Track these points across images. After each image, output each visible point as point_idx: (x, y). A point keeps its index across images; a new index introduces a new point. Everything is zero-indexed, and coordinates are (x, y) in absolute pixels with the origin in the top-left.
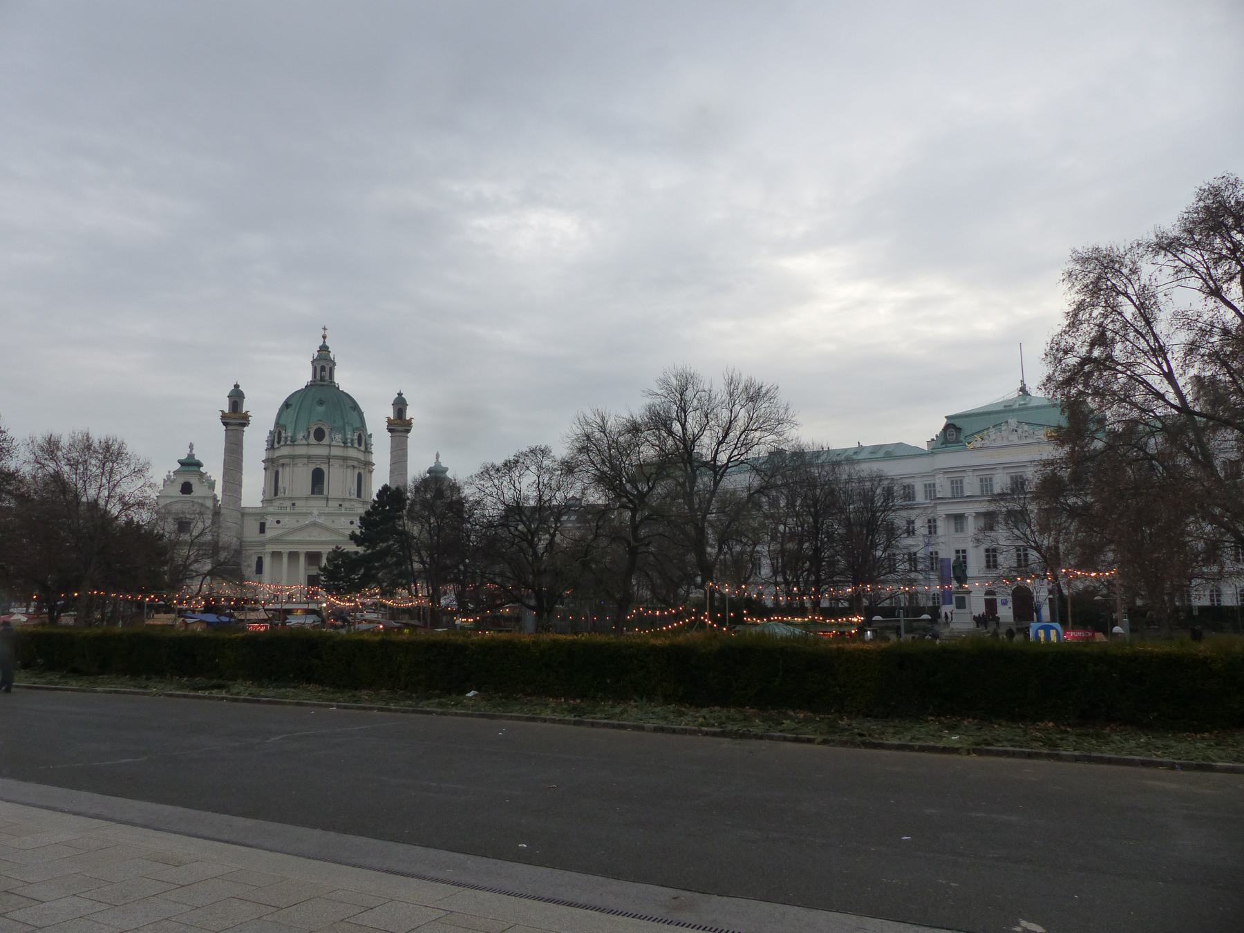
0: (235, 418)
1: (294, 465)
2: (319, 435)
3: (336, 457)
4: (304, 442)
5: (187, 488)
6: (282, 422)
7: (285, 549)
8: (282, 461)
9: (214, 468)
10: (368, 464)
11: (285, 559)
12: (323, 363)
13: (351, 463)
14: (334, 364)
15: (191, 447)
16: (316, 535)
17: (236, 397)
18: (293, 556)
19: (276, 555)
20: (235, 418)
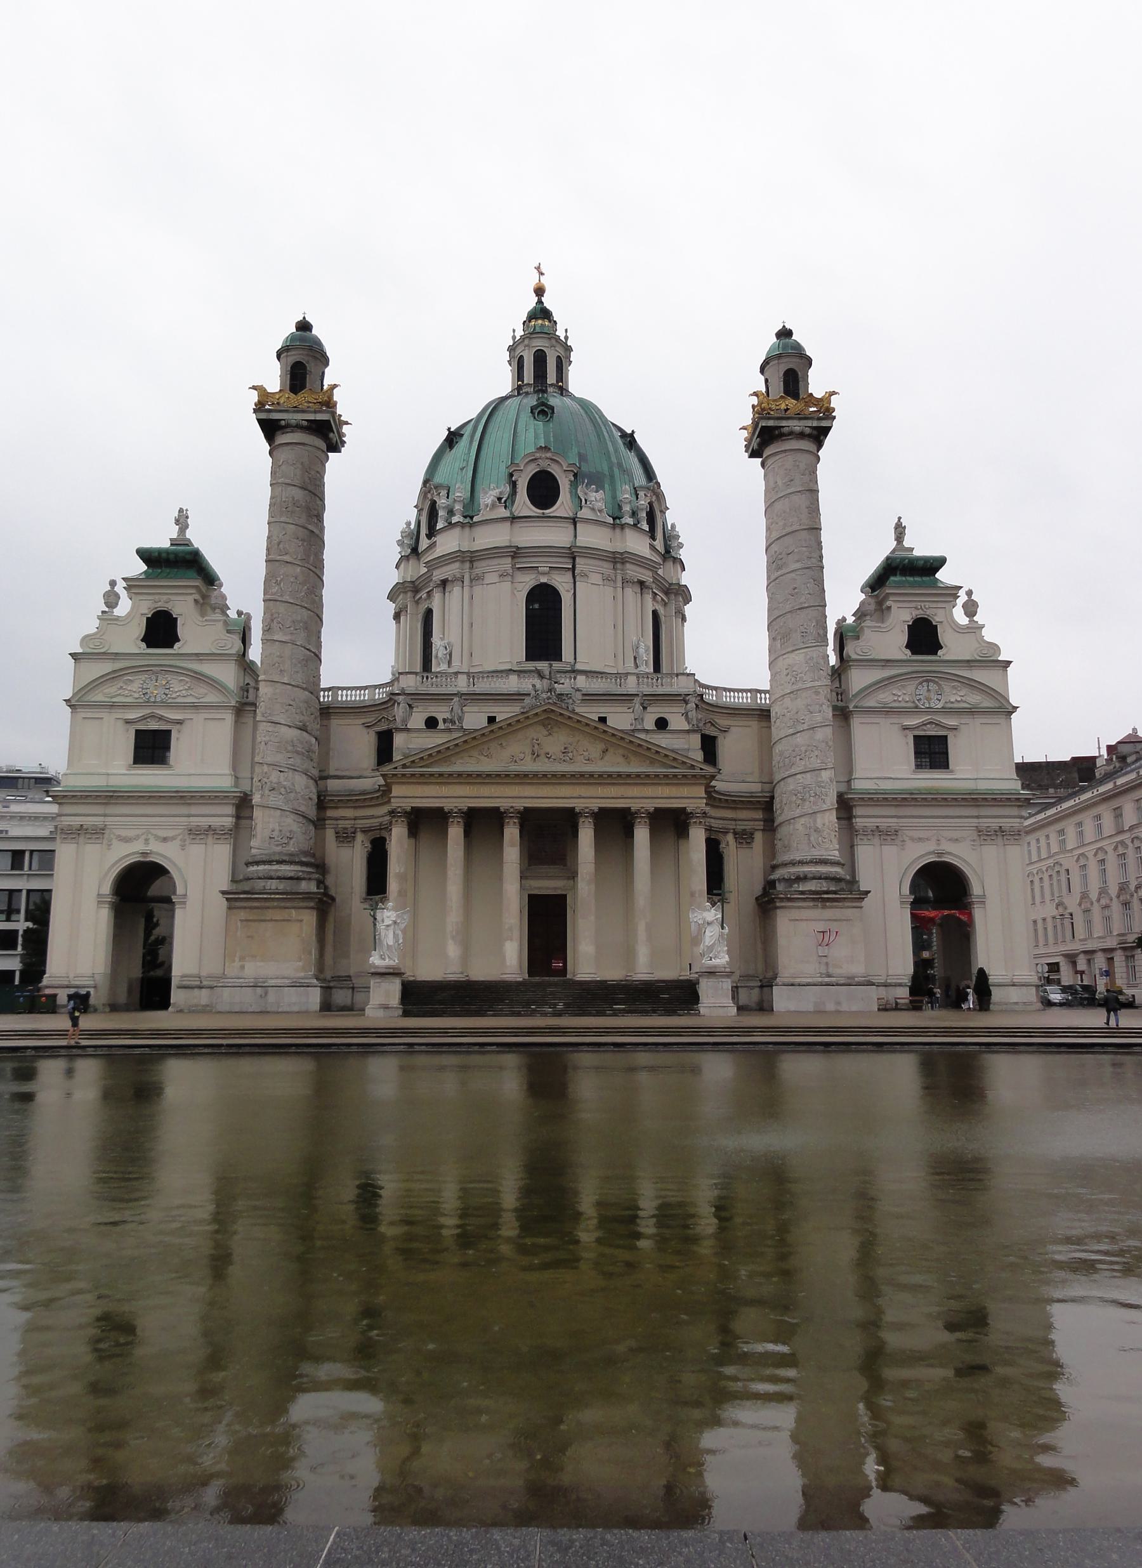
0: (301, 415)
1: (476, 579)
2: (543, 490)
4: (503, 512)
5: (161, 630)
6: (438, 479)
7: (455, 798)
8: (439, 575)
9: (243, 584)
11: (455, 832)
12: (539, 343)
14: (569, 349)
15: (182, 520)
16: (555, 750)
17: (303, 358)
18: (482, 824)
20: (301, 415)
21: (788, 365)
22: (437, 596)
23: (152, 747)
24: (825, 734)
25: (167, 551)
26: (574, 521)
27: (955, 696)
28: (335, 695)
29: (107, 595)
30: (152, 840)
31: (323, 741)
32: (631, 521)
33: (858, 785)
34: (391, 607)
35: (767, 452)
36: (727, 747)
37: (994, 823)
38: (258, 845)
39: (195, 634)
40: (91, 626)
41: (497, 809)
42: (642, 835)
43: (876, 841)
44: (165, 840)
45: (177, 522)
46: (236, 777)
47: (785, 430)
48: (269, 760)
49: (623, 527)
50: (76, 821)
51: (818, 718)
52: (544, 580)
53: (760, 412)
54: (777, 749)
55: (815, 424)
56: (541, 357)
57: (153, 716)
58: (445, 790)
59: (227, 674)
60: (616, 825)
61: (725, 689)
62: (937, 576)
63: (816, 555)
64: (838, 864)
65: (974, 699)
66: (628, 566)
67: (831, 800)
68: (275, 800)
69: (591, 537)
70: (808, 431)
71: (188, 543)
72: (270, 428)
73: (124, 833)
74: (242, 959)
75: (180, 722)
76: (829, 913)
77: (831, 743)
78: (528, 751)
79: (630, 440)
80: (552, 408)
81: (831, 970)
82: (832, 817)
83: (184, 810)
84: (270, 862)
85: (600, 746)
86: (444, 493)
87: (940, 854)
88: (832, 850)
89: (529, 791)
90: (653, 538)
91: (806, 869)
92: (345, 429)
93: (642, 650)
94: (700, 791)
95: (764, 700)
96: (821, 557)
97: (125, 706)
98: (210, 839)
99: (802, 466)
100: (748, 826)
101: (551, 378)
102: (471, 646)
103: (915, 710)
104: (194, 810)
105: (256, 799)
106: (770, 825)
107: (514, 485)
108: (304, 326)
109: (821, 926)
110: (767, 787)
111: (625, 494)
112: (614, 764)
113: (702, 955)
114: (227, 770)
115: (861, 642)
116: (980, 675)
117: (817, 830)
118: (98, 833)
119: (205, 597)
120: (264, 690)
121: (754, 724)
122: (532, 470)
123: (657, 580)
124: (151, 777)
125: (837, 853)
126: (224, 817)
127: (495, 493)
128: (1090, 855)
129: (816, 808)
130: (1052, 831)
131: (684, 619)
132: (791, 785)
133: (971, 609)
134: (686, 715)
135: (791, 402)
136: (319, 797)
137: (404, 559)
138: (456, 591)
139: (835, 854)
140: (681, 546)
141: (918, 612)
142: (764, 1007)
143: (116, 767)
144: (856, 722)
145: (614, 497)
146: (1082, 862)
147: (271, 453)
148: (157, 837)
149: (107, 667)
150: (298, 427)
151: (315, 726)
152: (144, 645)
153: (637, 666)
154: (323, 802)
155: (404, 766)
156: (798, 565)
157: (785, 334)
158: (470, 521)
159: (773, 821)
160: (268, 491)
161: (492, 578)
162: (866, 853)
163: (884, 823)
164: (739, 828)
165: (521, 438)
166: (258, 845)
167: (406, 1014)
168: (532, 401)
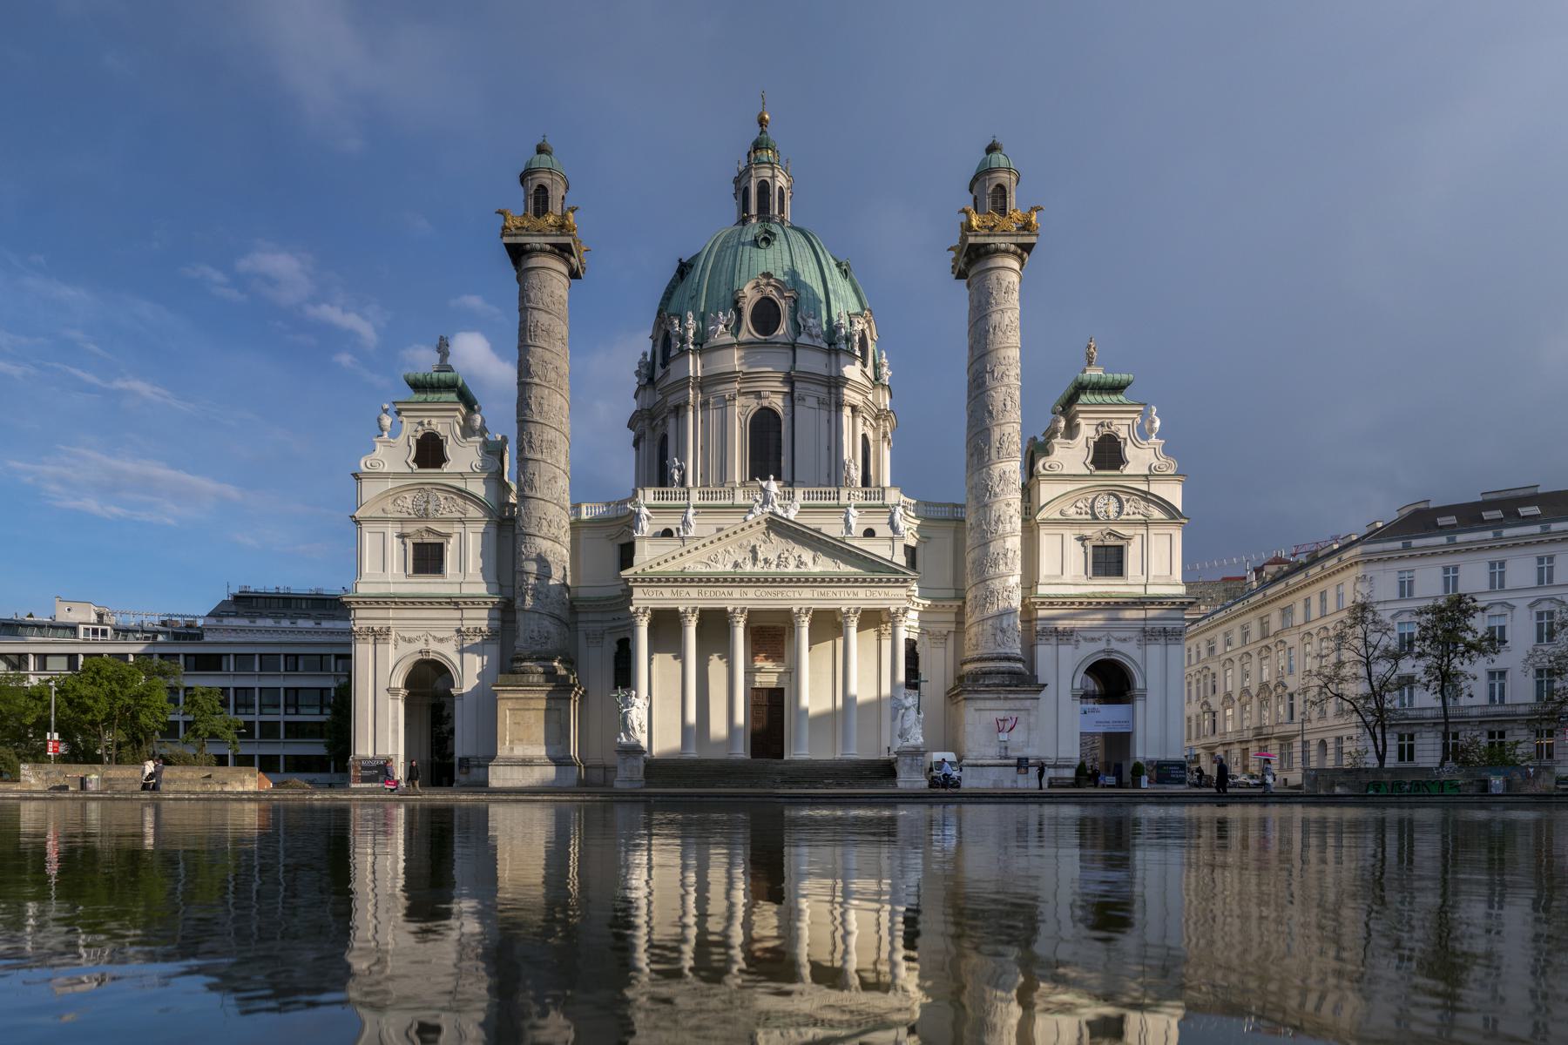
3: (810, 377)
7: (688, 601)
24: (1014, 543)
26: (793, 347)
33: (1042, 590)
44: (441, 640)
52: (765, 403)
57: (429, 531)
60: (828, 625)
64: (1019, 660)
73: (407, 635)
83: (457, 614)
89: (751, 593)
91: (991, 664)
97: (402, 521)
100: (944, 628)
107: (739, 312)
117: (1003, 631)
134: (892, 524)
137: (641, 388)
139: (1016, 649)
152: (415, 466)
159: (963, 623)
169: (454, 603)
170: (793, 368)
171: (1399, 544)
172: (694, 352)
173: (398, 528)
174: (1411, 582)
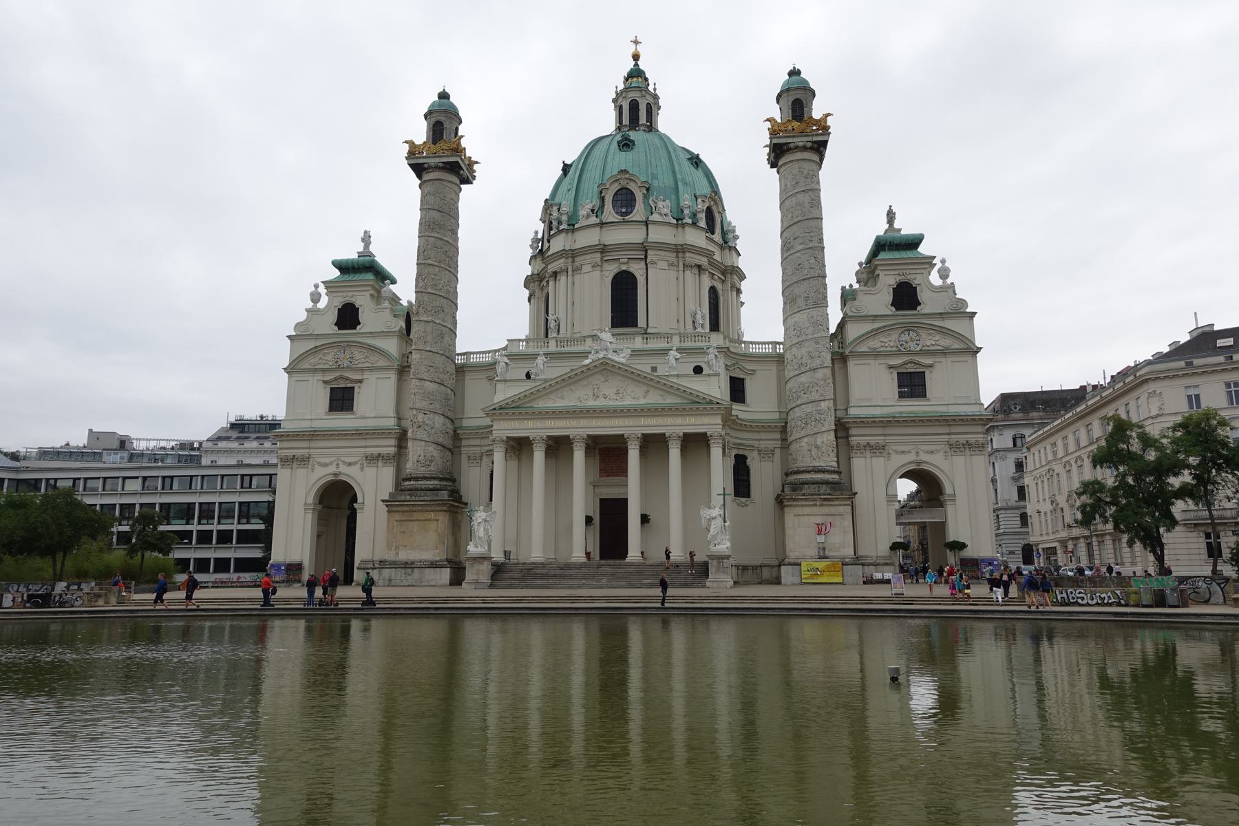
0: (441, 161)
1: (576, 270)
2: (625, 200)
3: (660, 246)
4: (594, 220)
5: (348, 317)
6: (557, 200)
7: (537, 430)
8: (552, 267)
10: (733, 274)
13: (691, 258)
14: (656, 97)
15: (366, 239)
16: (611, 394)
17: (443, 119)
19: (519, 447)
20: (441, 161)
21: (796, 97)
22: (551, 283)
23: (342, 399)
25: (358, 262)
26: (646, 223)
27: (929, 341)
28: (468, 359)
29: (312, 294)
30: (341, 465)
31: (458, 392)
32: (690, 221)
33: (853, 412)
34: (527, 293)
35: (780, 163)
36: (752, 388)
37: (962, 439)
38: (410, 467)
39: (371, 318)
40: (303, 316)
41: (568, 437)
42: (675, 453)
43: (868, 454)
45: (363, 240)
46: (399, 419)
47: (792, 146)
48: (418, 405)
49: (683, 225)
50: (290, 453)
51: (817, 362)
52: (624, 268)
53: (773, 133)
54: (790, 385)
55: (815, 139)
56: (636, 106)
57: (342, 378)
58: (530, 424)
59: (391, 346)
61: (752, 343)
62: (919, 250)
63: (816, 239)
64: (834, 472)
65: (946, 342)
66: (687, 254)
67: (830, 424)
68: (421, 434)
69: (659, 235)
70: (809, 145)
71: (371, 255)
72: (419, 169)
74: (397, 548)
75: (360, 381)
76: (825, 510)
77: (830, 381)
78: (590, 393)
79: (696, 161)
80: (633, 142)
81: (827, 553)
82: (832, 436)
83: (363, 443)
84: (416, 479)
85: (645, 388)
86: (555, 208)
87: (919, 463)
88: (830, 461)
90: (713, 233)
91: (808, 476)
92: (476, 167)
93: (698, 317)
94: (719, 420)
95: (780, 349)
96: (821, 240)
97: (323, 371)
98: (380, 464)
99: (806, 172)
100: (770, 445)
101: (643, 119)
102: (573, 319)
103: (898, 353)
104: (370, 443)
105: (410, 434)
106: (785, 444)
107: (603, 199)
108: (444, 96)
109: (819, 520)
110: (784, 416)
111: (686, 200)
112: (656, 398)
113: (709, 542)
114: (392, 413)
115: (856, 303)
116: (949, 324)
118: (305, 460)
119: (379, 292)
120: (415, 356)
121: (774, 368)
122: (616, 187)
123: (712, 263)
124: (342, 421)
125: (835, 464)
126: (388, 447)
127: (590, 206)
128: (1073, 462)
129: (816, 430)
130: (1047, 443)
131: (739, 291)
132: (798, 413)
133: (944, 274)
135: (796, 124)
136: (455, 431)
138: (562, 279)
140: (736, 237)
141: (899, 278)
142: (777, 581)
143: (317, 413)
144: (851, 364)
145: (678, 204)
146: (1068, 468)
147: (420, 186)
148: (344, 462)
149: (311, 345)
150: (437, 168)
151: (450, 383)
153: (695, 328)
154: (456, 437)
155: (501, 408)
156: (802, 247)
157: (794, 73)
158: (572, 228)
160: (417, 215)
161: (586, 268)
162: (859, 464)
163: (873, 440)
164: (763, 445)
165: (609, 167)
166: (410, 467)
167: (491, 586)
168: (619, 138)
169: (359, 434)
170: (646, 240)
171: (1182, 364)
172: (567, 231)
173: (320, 377)
174: (1197, 396)
